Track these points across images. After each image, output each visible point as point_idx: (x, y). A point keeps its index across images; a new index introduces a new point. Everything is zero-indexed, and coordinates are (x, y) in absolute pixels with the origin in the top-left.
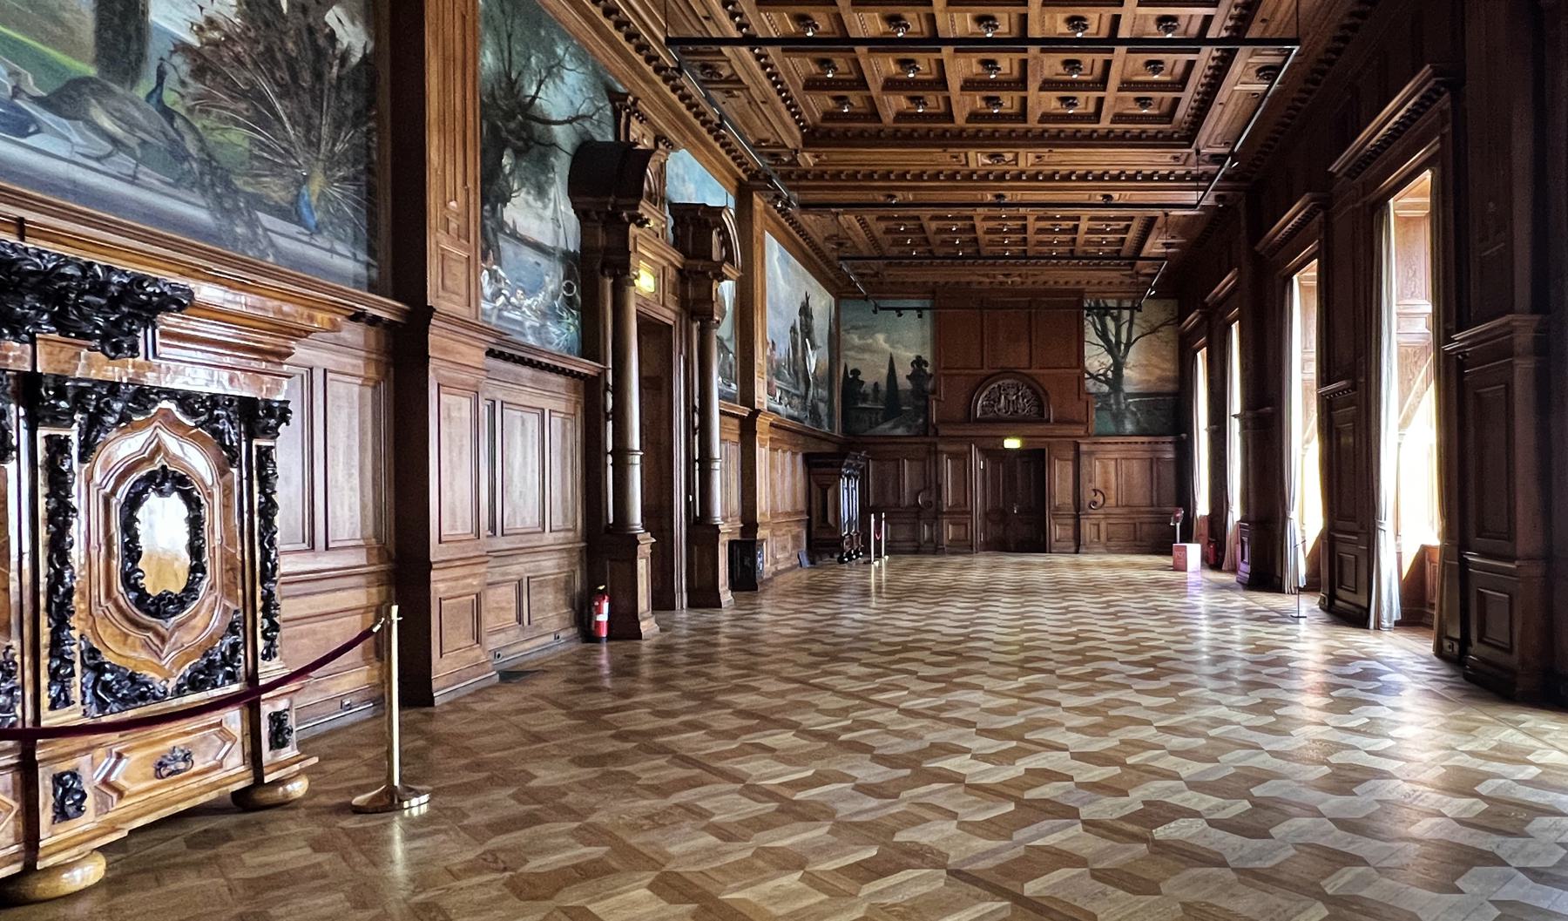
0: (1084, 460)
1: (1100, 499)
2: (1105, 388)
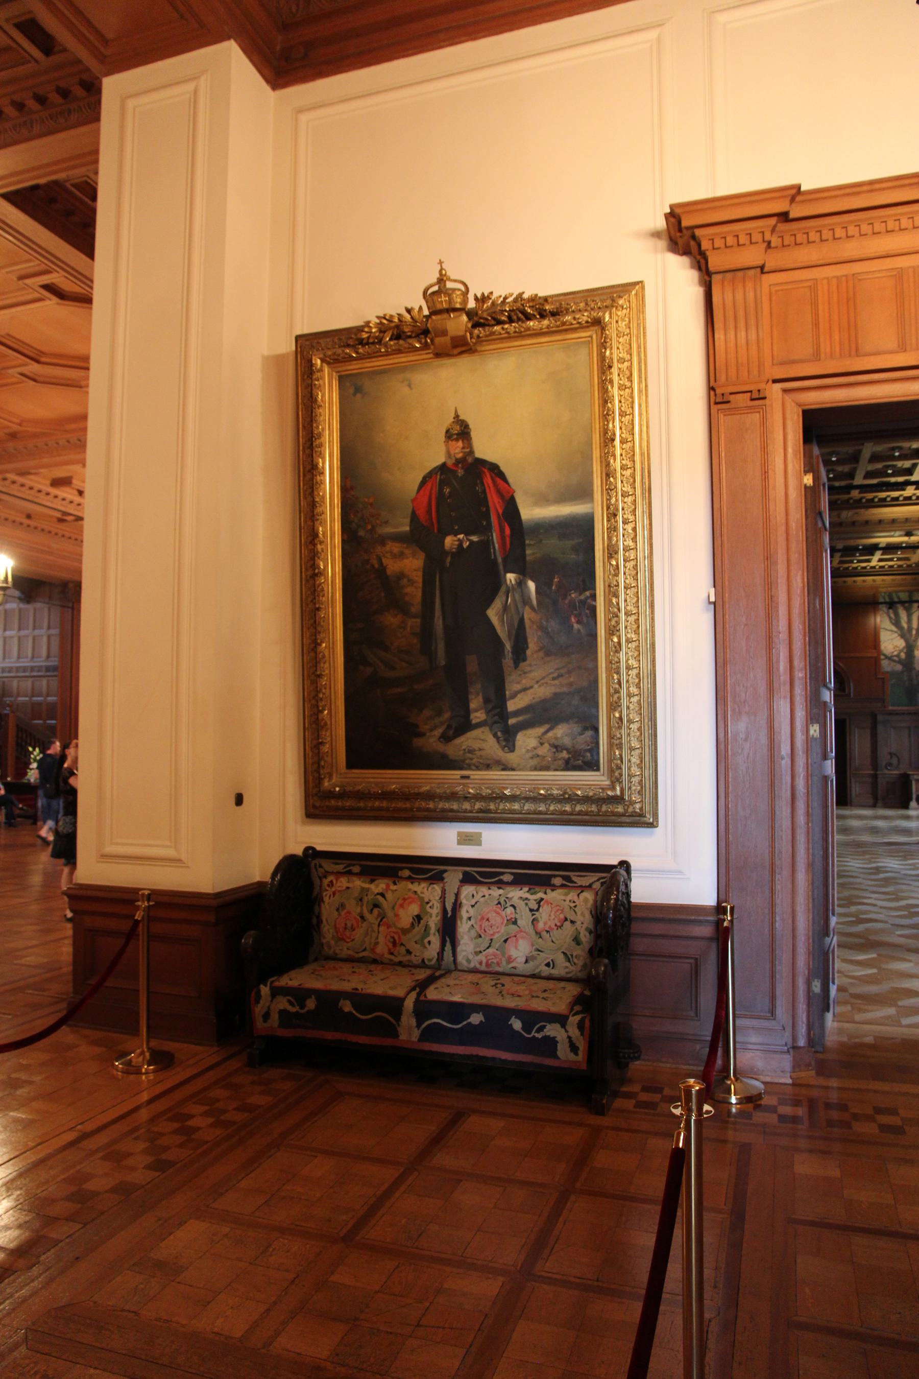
0: (880, 729)
1: (895, 761)
2: (899, 667)
